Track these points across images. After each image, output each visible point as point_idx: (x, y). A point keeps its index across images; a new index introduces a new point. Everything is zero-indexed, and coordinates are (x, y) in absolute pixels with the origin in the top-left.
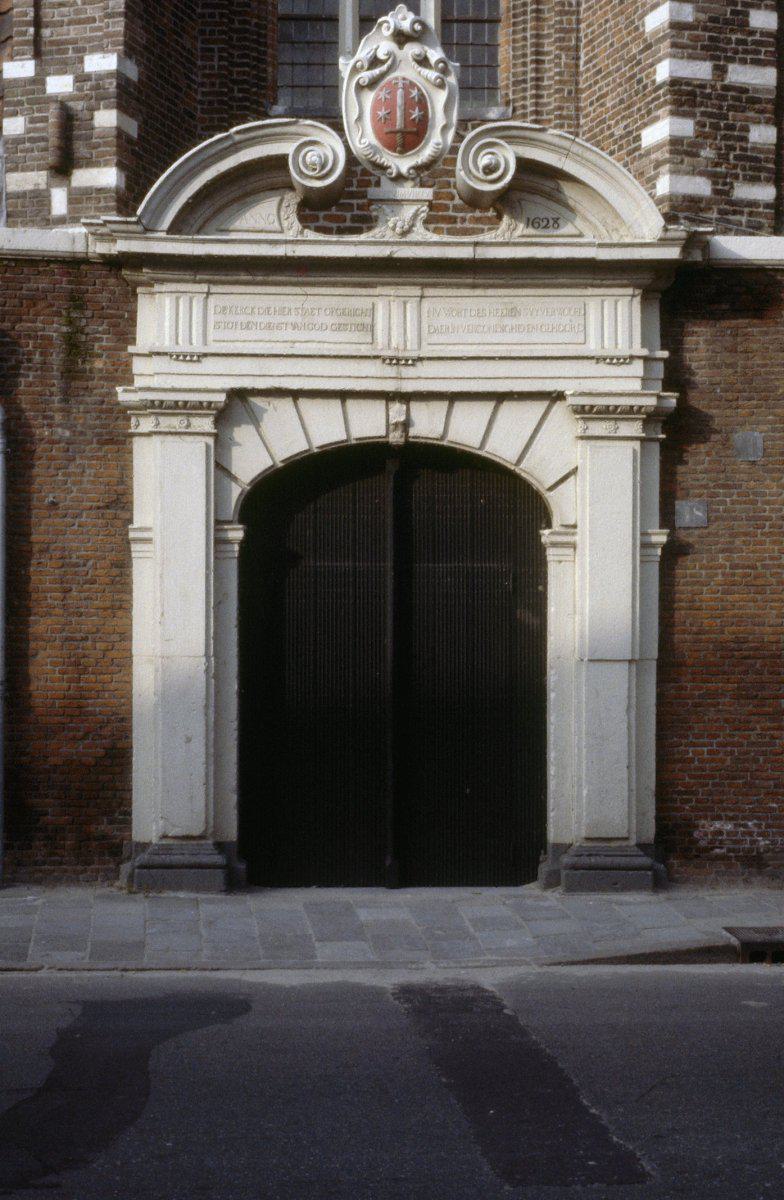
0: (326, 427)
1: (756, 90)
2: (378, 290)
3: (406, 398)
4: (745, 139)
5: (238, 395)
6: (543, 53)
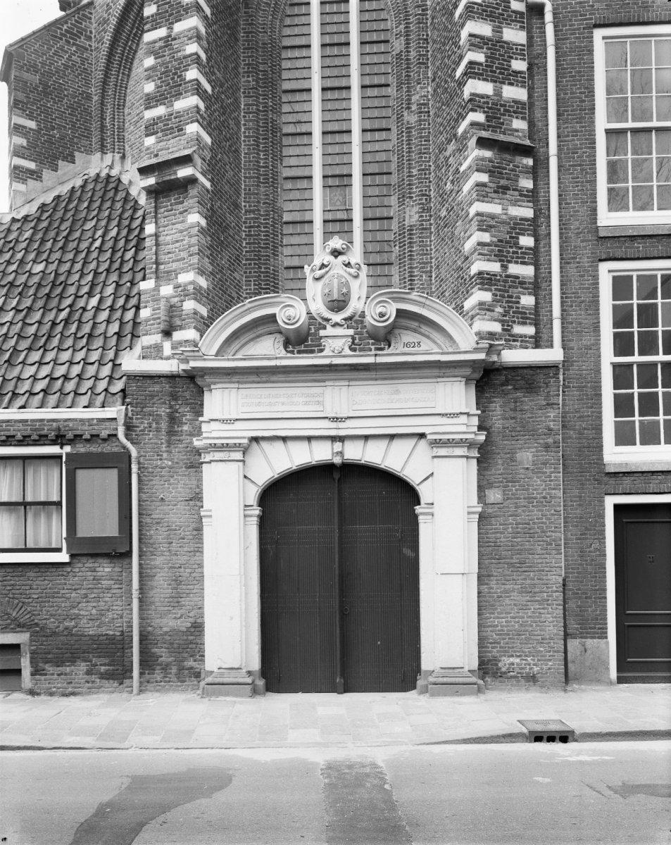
0: (302, 456)
1: (524, 278)
2: (327, 383)
3: (342, 439)
4: (518, 302)
5: (256, 440)
6: (414, 276)
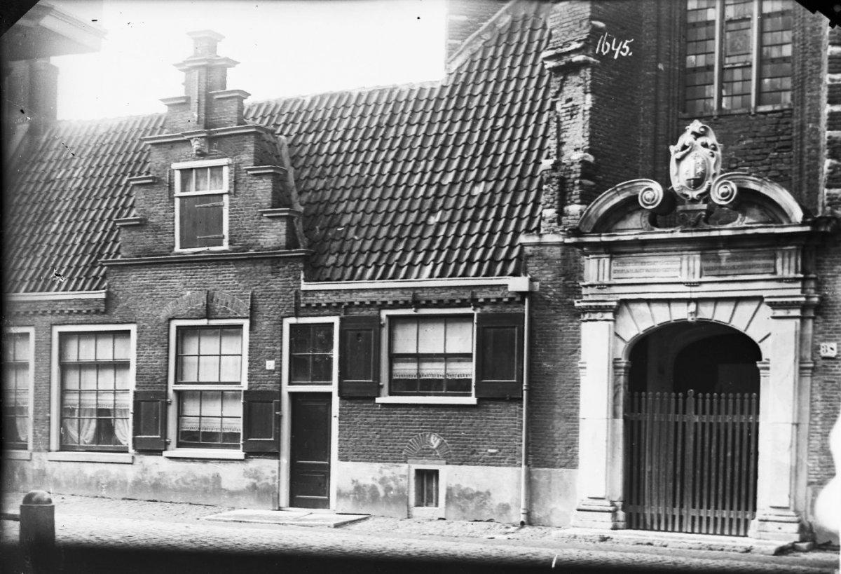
0: (662, 315)
